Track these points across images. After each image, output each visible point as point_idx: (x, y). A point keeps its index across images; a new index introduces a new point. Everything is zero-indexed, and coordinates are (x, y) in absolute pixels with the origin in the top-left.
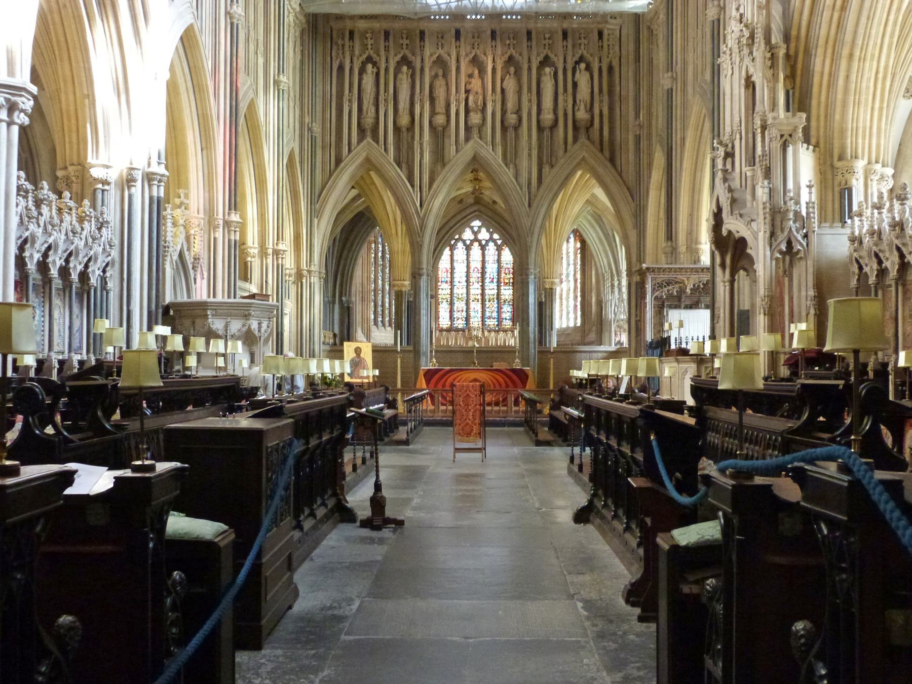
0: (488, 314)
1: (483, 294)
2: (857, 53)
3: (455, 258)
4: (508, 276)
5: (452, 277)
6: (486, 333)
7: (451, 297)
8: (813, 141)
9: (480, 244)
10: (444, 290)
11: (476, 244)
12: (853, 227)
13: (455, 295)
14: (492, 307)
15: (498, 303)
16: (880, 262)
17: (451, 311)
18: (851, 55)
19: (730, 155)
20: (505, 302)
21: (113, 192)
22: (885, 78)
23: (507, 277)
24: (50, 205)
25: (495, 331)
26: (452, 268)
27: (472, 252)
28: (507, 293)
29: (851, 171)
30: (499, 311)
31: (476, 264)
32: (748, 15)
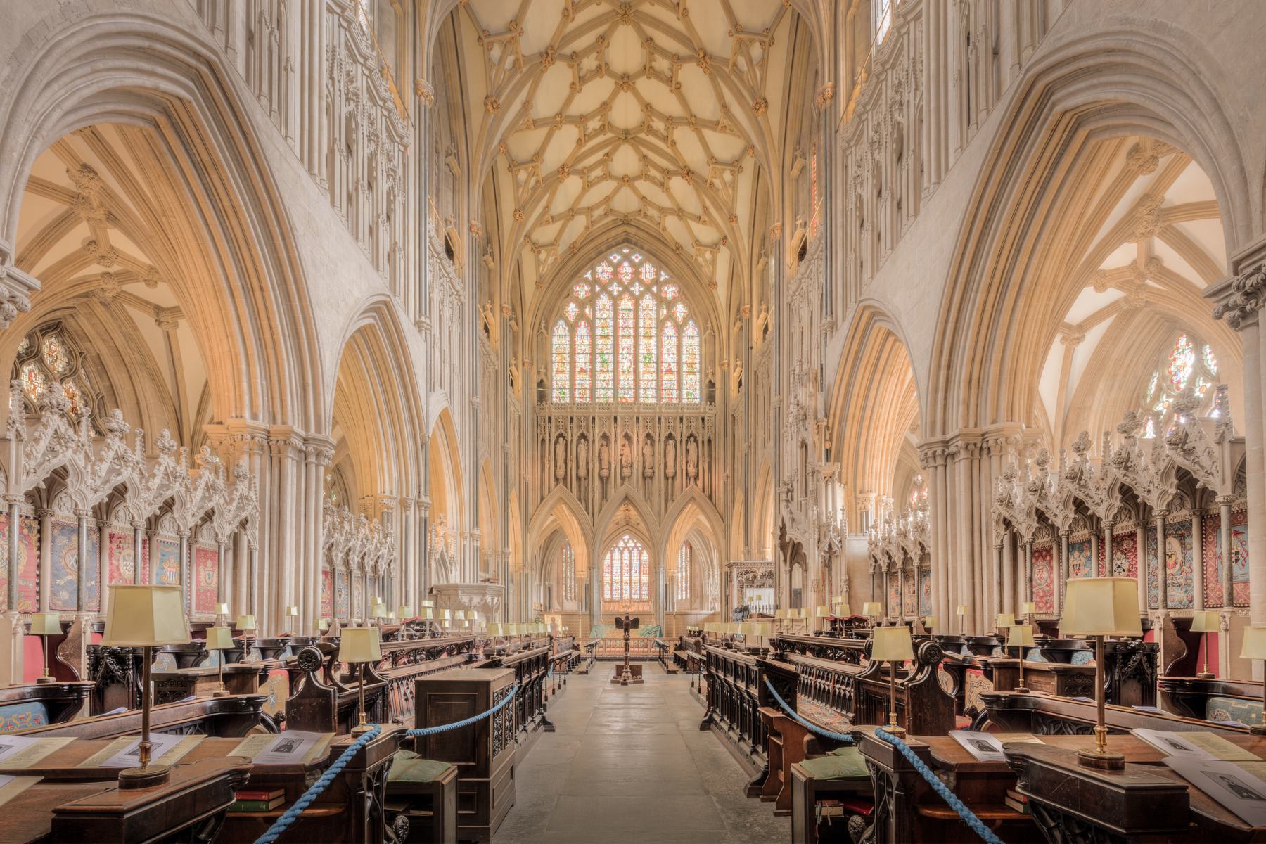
1: (630, 580)
2: (873, 424)
8: (844, 481)
10: (607, 577)
12: (870, 536)
14: (636, 588)
16: (890, 557)
17: (612, 590)
18: (869, 426)
19: (790, 491)
21: (394, 514)
22: (889, 441)
23: (646, 569)
24: (350, 521)
26: (612, 564)
28: (645, 579)
29: (868, 500)
30: (640, 591)
31: (626, 562)
32: (803, 401)
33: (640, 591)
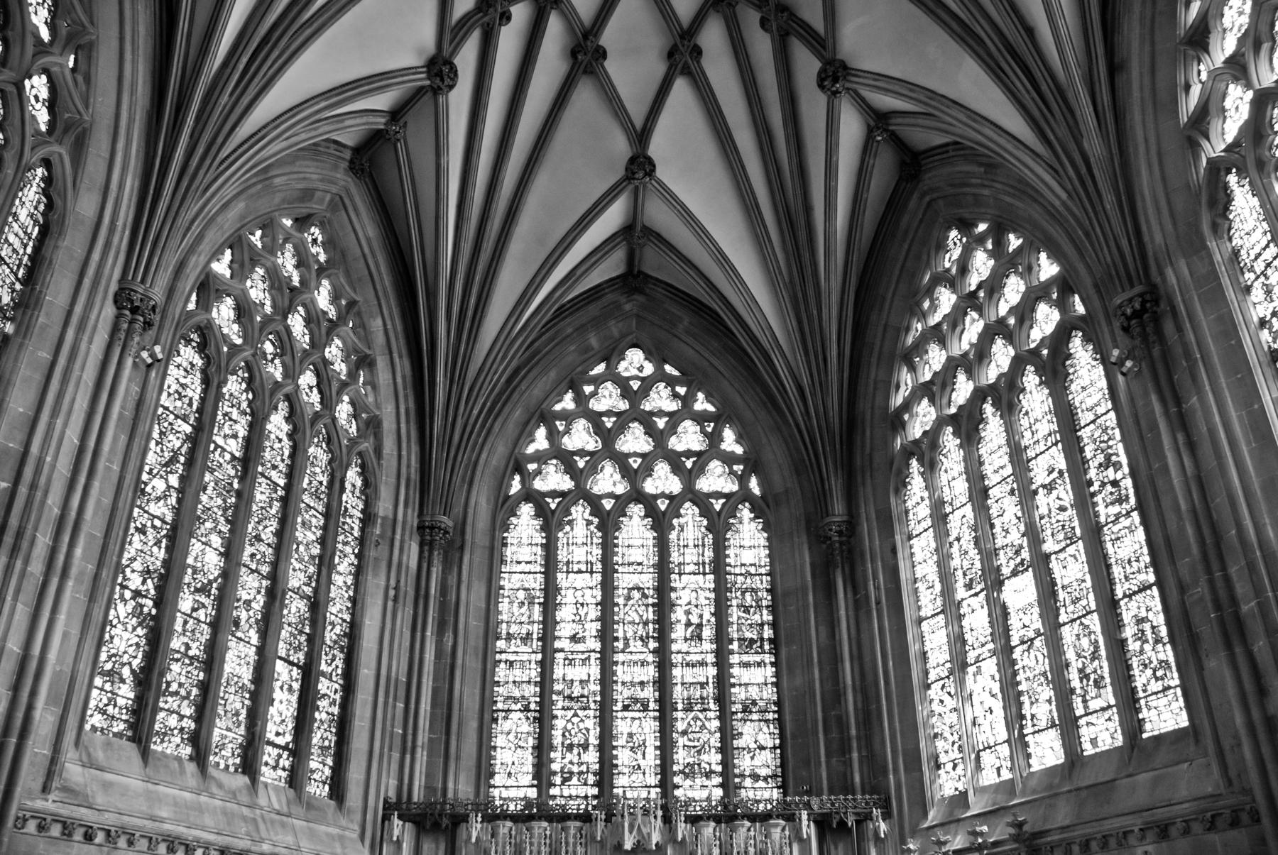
0: (682, 757)
1: (663, 683)
3: (562, 555)
4: (757, 617)
5: (549, 623)
6: (682, 829)
7: (541, 695)
9: (651, 511)
11: (636, 510)
13: (557, 687)
15: (725, 716)
17: (542, 748)
20: (746, 710)
25: (718, 820)
26: (551, 591)
27: (623, 537)
30: (727, 750)
33: (727, 750)
